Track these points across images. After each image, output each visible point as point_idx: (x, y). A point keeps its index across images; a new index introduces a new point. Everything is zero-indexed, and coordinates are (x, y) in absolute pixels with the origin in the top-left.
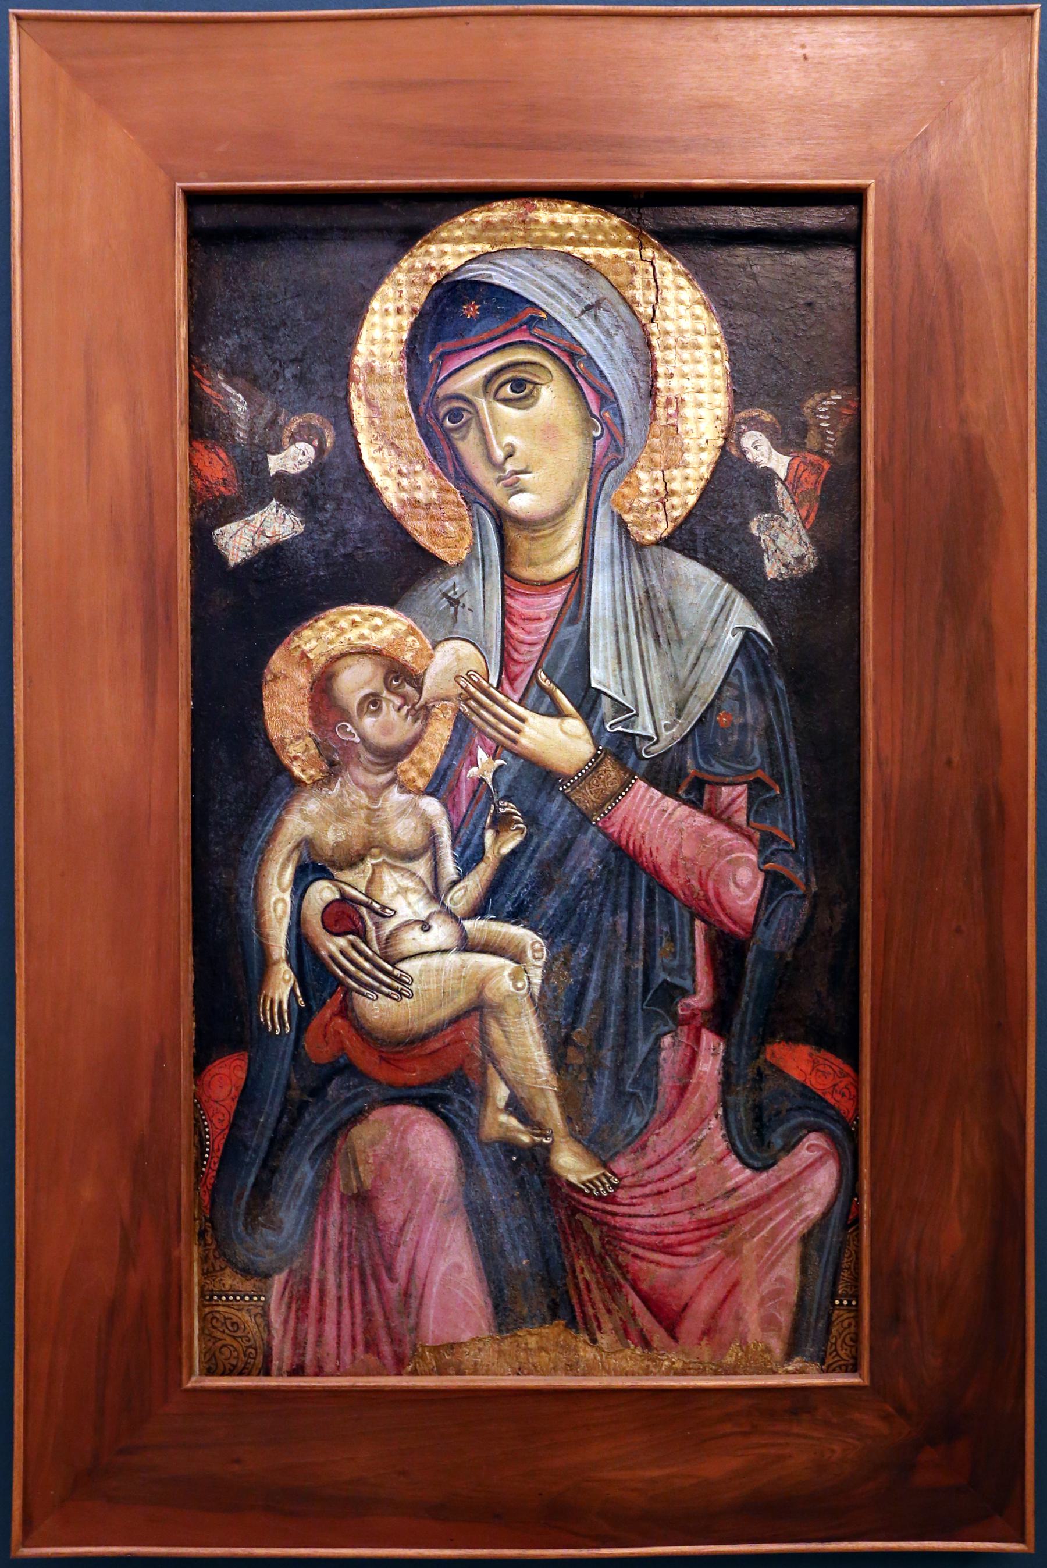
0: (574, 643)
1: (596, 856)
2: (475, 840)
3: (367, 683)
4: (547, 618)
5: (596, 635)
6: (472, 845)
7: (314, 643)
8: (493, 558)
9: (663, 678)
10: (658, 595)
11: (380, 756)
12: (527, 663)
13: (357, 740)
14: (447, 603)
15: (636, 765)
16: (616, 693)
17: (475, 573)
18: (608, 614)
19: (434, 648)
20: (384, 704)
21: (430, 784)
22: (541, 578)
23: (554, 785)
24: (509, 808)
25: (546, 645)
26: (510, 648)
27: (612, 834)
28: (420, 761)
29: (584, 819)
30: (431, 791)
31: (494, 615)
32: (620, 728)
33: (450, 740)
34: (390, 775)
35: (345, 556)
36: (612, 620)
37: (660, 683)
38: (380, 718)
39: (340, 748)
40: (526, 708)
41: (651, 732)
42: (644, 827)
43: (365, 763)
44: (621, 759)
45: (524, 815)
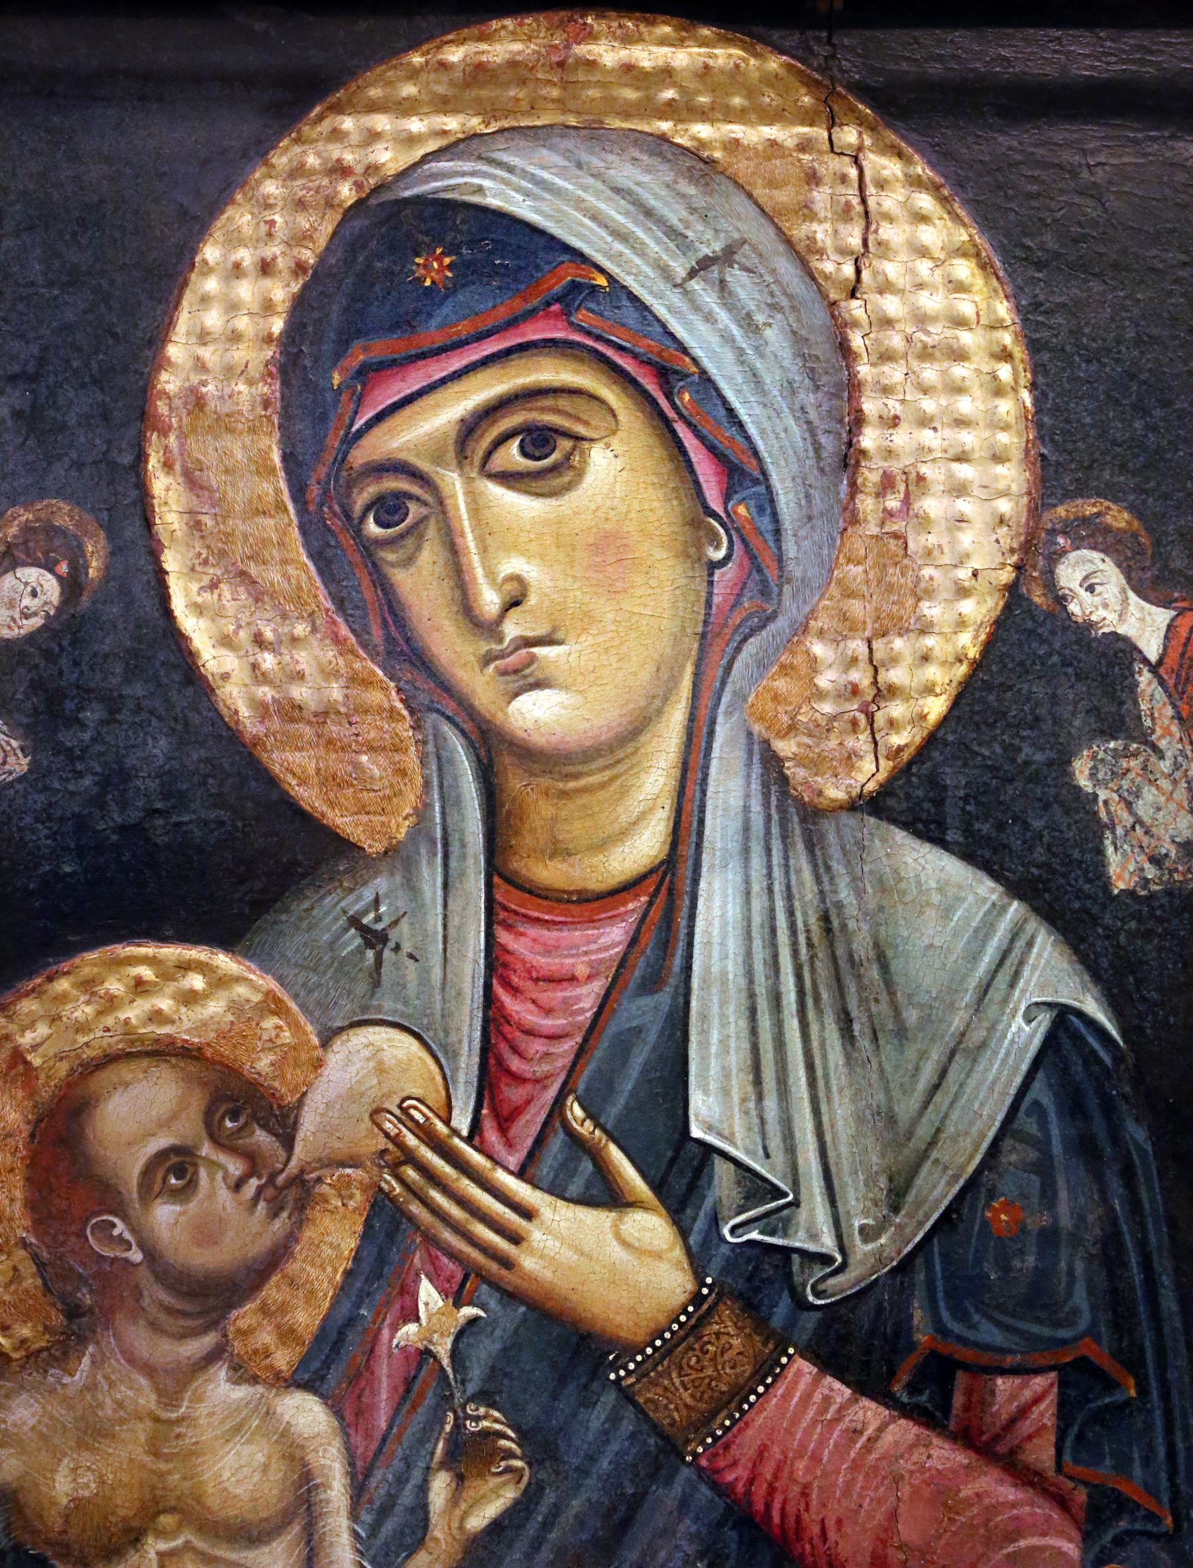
0: (652, 1036)
1: (693, 1537)
2: (407, 1498)
3: (165, 1124)
4: (590, 978)
5: (704, 1017)
6: (398, 1509)
7: (43, 1030)
8: (470, 839)
9: (860, 1119)
10: (852, 925)
11: (190, 1295)
12: (541, 1082)
13: (136, 1256)
14: (358, 941)
15: (791, 1323)
16: (747, 1152)
17: (425, 872)
18: (733, 968)
19: (326, 1043)
20: (203, 1173)
21: (304, 1362)
22: (579, 885)
23: (598, 1367)
24: (491, 1420)
25: (585, 1040)
26: (504, 1049)
27: (732, 1486)
28: (284, 1308)
29: (666, 1450)
30: (307, 1378)
31: (468, 969)
32: (755, 1235)
33: (356, 1259)
34: (209, 1340)
35: (122, 829)
36: (743, 982)
37: (852, 1131)
38: (193, 1206)
39: (95, 1276)
40: (536, 1186)
41: (827, 1243)
42: (807, 1469)
43: (153, 1311)
44: (756, 1308)
45: (523, 1437)
